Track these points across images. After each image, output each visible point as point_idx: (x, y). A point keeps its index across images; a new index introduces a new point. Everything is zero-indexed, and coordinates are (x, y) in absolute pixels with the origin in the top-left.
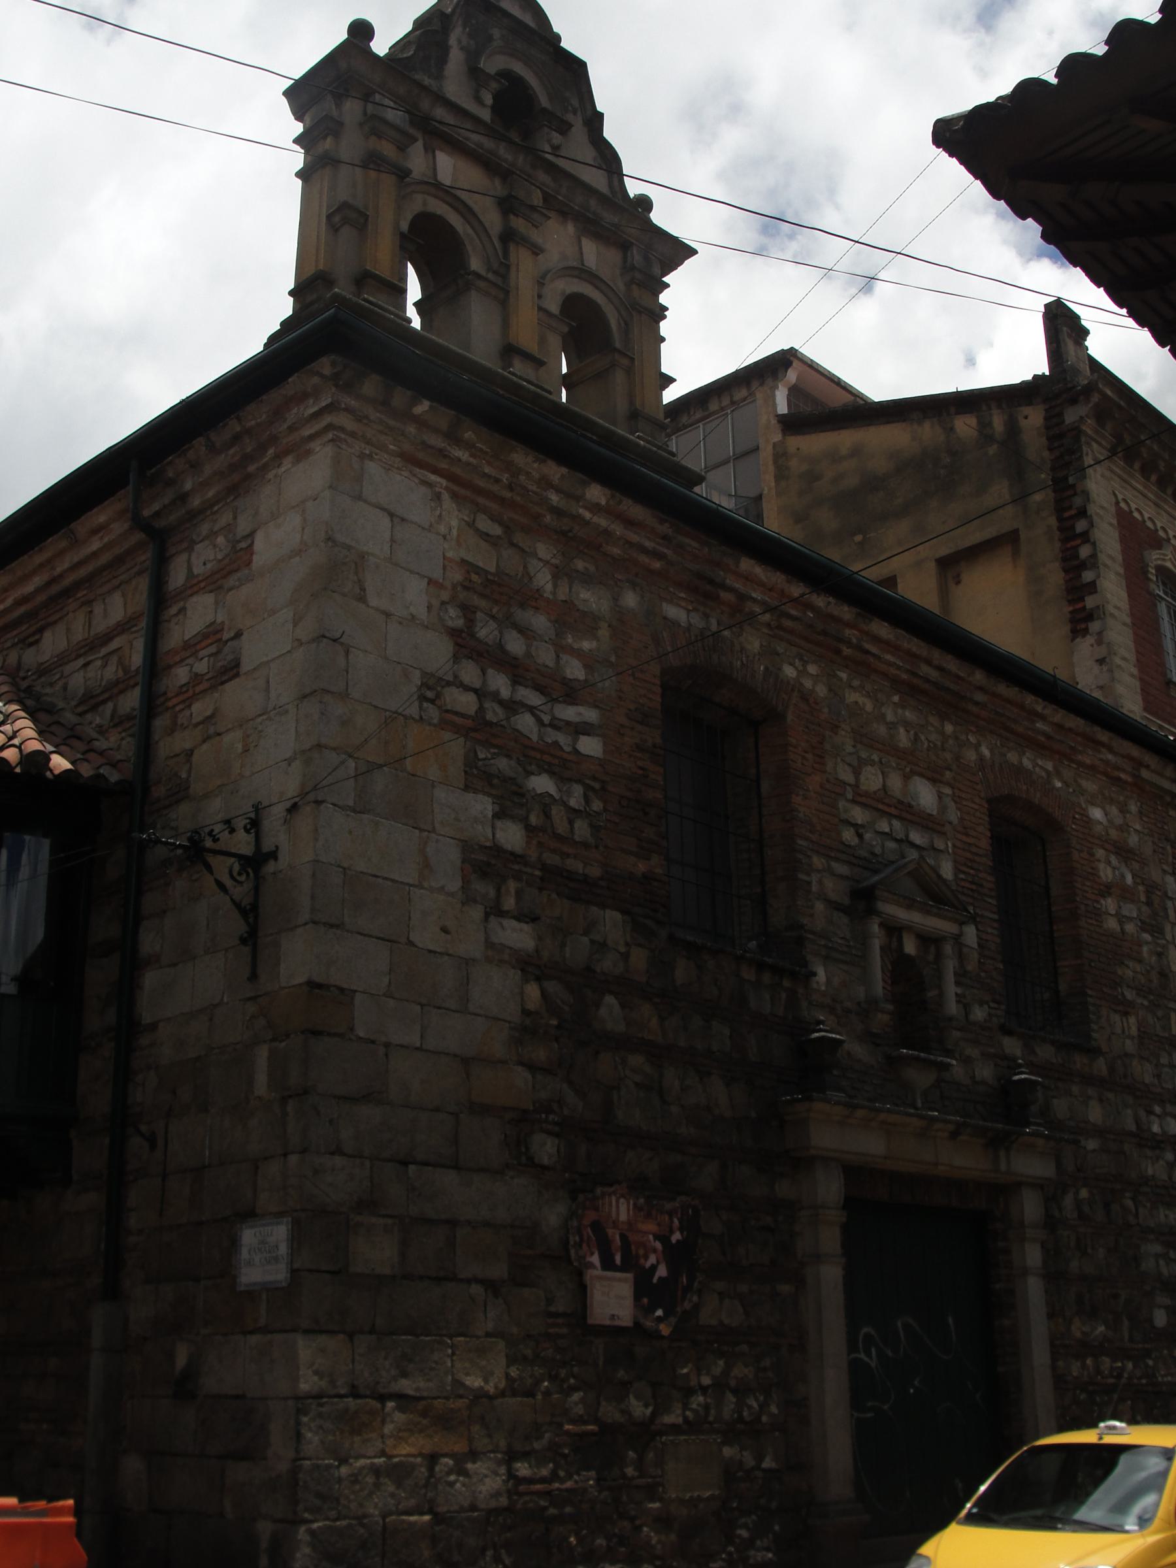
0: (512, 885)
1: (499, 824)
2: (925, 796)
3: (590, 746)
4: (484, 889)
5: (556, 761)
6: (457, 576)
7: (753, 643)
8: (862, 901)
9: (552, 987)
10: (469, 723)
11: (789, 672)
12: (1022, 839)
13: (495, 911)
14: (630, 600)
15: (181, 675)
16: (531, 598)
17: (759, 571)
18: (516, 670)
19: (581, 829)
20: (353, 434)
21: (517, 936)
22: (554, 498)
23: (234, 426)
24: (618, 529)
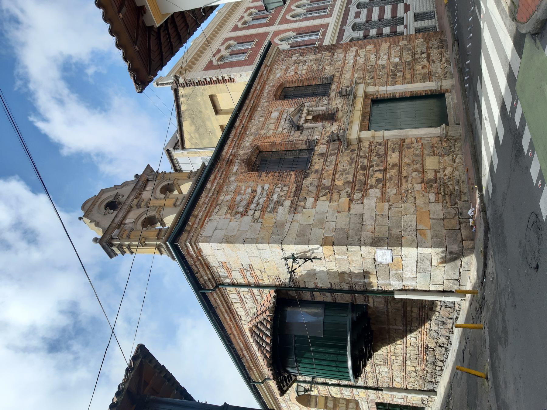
2: (275, 115)
3: (267, 187)
4: (299, 209)
6: (229, 215)
7: (241, 152)
8: (299, 128)
11: (248, 144)
12: (285, 93)
13: (304, 207)
14: (232, 179)
16: (233, 199)
17: (225, 150)
18: (250, 203)
19: (285, 188)
20: (196, 238)
21: (310, 200)
22: (210, 195)
23: (193, 267)
24: (216, 181)
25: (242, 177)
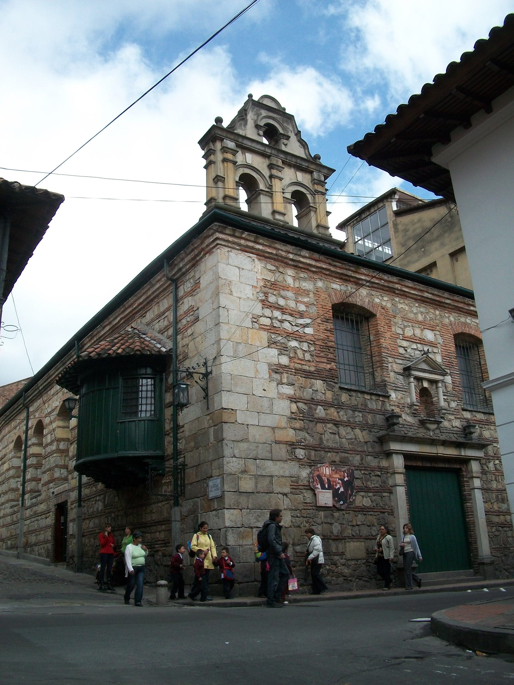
0: (285, 375)
1: (280, 357)
2: (429, 335)
3: (309, 331)
4: (277, 376)
5: (298, 336)
6: (262, 283)
8: (407, 371)
9: (300, 405)
10: (268, 328)
11: (377, 300)
13: (280, 383)
14: (320, 284)
15: (184, 322)
16: (286, 288)
18: (282, 310)
19: (308, 357)
20: (225, 246)
21: (289, 391)
24: (313, 263)
25: (323, 296)
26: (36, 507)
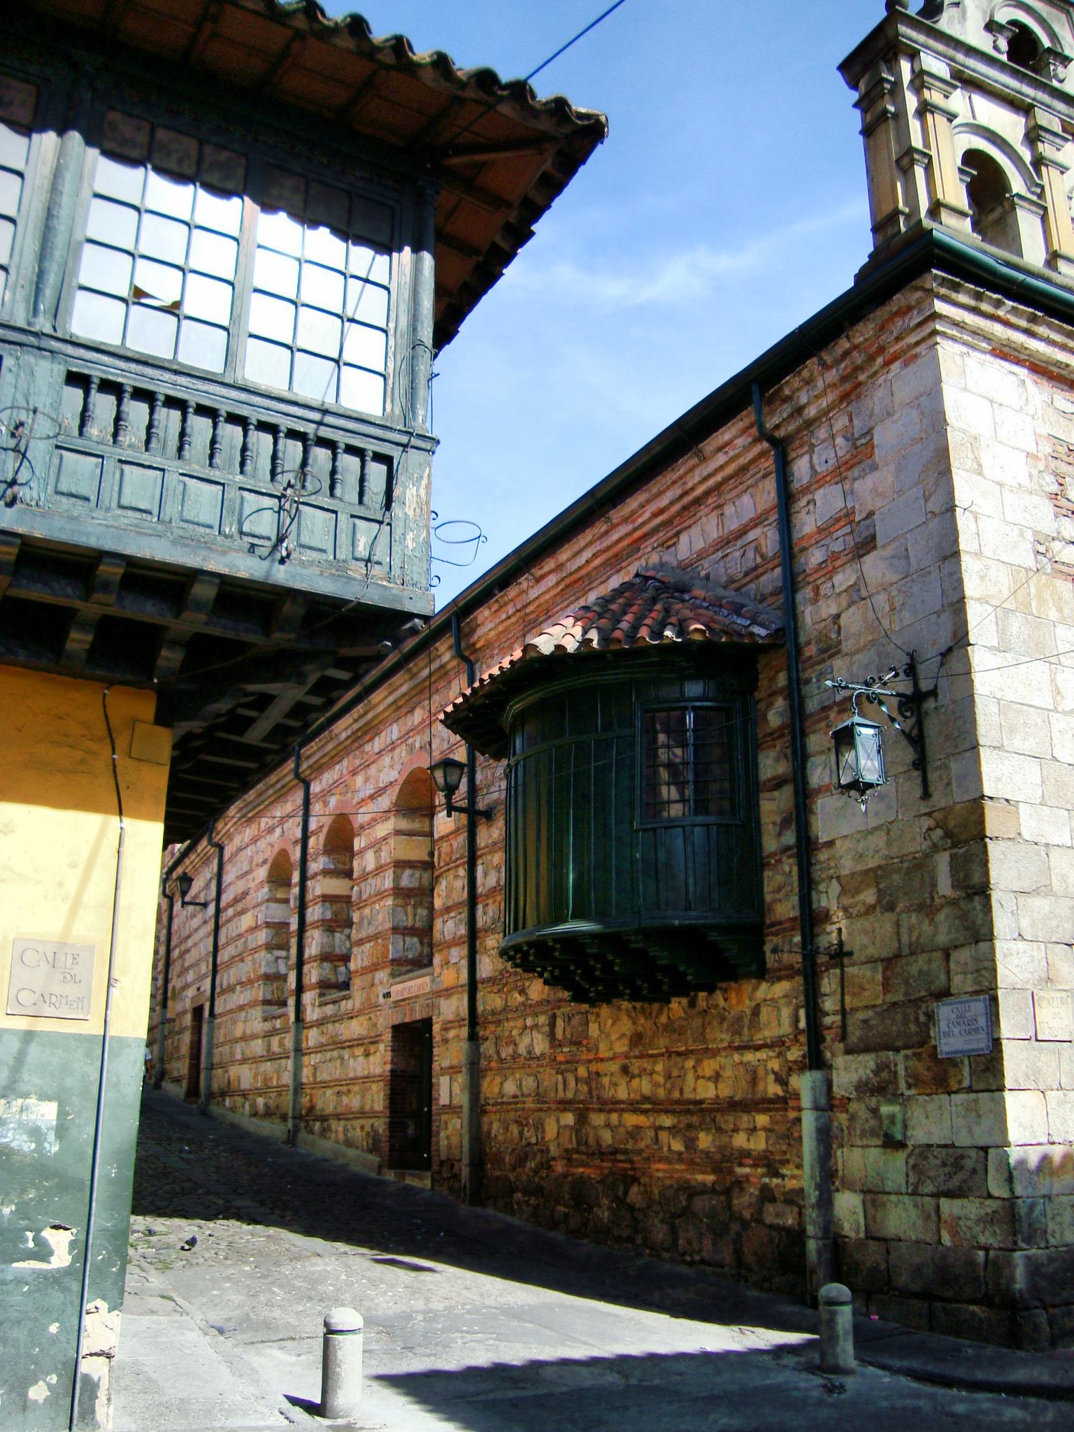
26: (337, 1025)
